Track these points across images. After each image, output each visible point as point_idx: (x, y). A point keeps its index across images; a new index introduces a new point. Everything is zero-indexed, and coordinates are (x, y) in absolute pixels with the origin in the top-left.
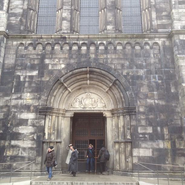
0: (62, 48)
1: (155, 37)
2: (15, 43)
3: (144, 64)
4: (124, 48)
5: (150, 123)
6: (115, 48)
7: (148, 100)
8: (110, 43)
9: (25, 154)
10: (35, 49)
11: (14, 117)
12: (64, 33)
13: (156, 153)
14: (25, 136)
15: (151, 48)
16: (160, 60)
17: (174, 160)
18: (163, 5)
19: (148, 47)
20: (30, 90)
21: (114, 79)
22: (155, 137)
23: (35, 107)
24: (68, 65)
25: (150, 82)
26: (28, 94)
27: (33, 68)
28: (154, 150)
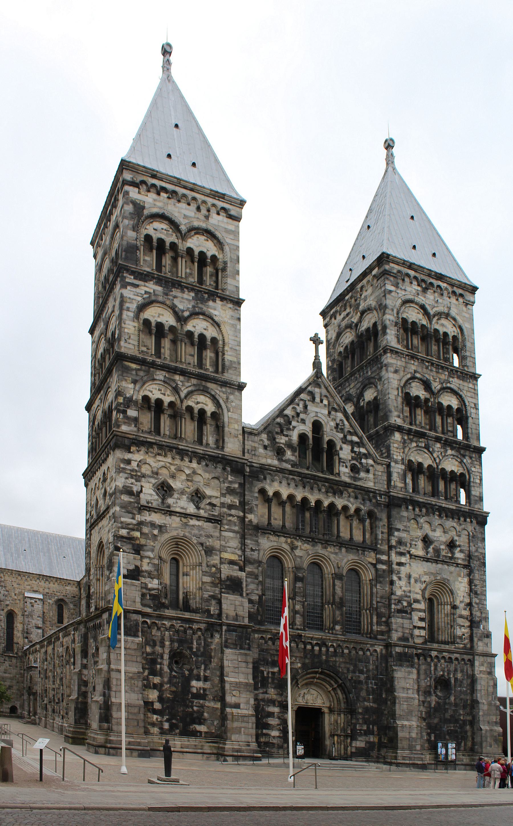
0: (297, 646)
1: (375, 644)
2: (256, 635)
3: (365, 669)
4: (350, 652)
5: (365, 722)
6: (343, 651)
7: (366, 703)
8: (339, 646)
9: (275, 741)
10: (274, 644)
11: (263, 709)
12: (298, 629)
13: (367, 745)
14: (274, 726)
15: (371, 654)
16: (377, 667)
17: (379, 750)
18: (383, 610)
19: (368, 653)
20: (273, 686)
21: (341, 682)
22: (368, 732)
23: (279, 702)
24: (304, 664)
25: (368, 687)
26: (273, 690)
27: (274, 664)
28: (367, 742)
